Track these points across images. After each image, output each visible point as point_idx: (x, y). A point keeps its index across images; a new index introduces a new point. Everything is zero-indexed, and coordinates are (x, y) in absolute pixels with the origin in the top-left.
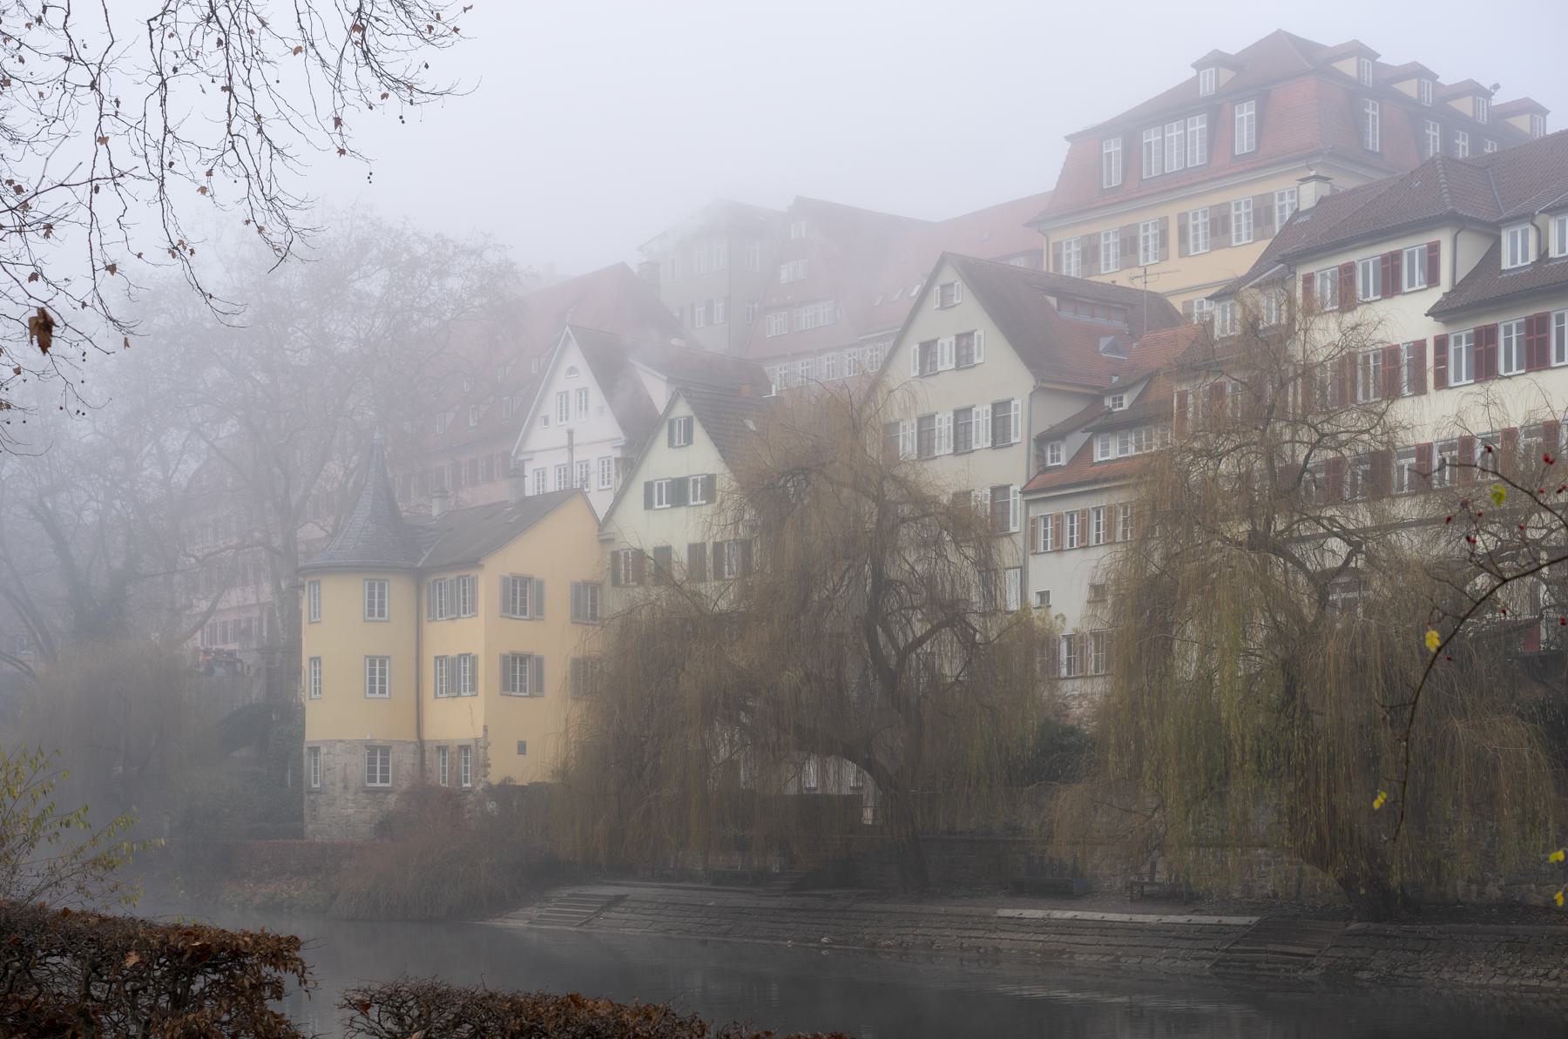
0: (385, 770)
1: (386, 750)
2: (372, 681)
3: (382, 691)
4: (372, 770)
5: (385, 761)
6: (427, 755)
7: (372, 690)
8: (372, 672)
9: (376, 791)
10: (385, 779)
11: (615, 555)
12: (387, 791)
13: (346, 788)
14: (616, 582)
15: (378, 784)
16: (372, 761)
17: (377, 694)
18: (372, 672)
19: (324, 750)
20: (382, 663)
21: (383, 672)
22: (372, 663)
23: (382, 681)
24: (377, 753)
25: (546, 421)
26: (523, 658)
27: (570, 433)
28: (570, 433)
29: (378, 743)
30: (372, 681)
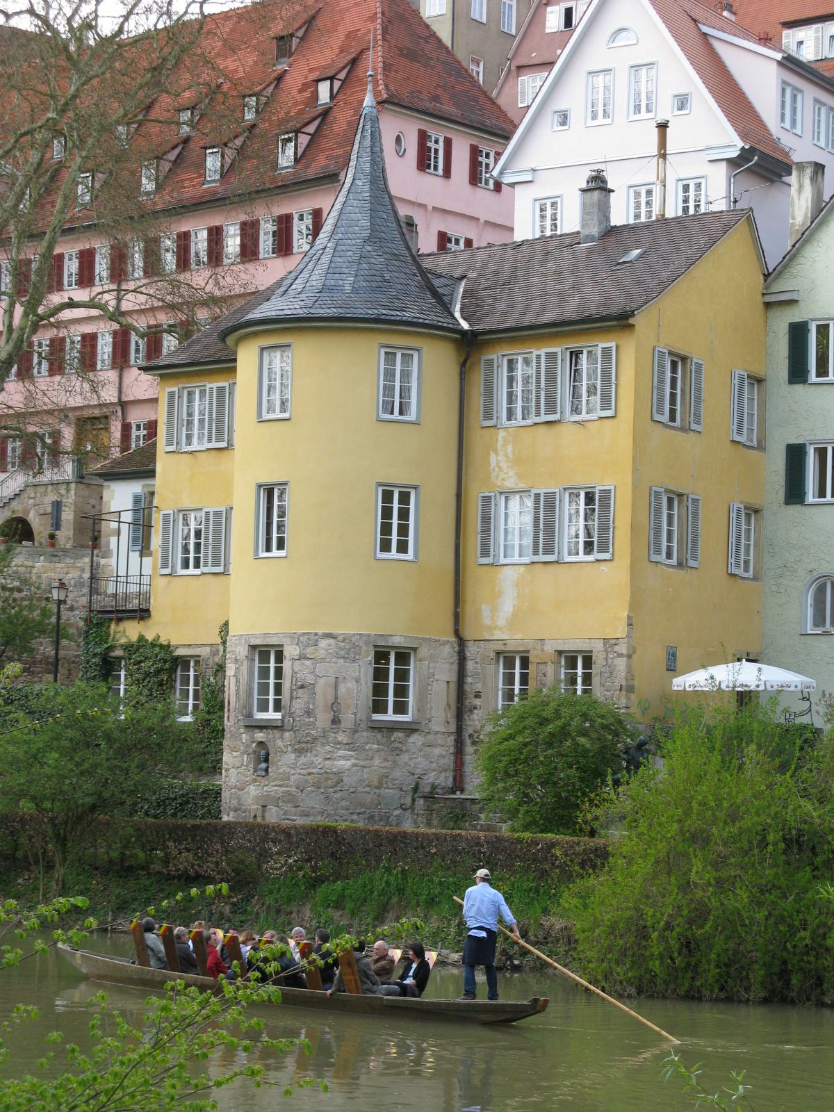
0: (401, 691)
1: (403, 657)
2: (386, 529)
3: (403, 547)
4: (379, 690)
5: (402, 676)
6: (470, 665)
7: (386, 546)
8: (387, 513)
9: (392, 728)
10: (400, 708)
11: (798, 332)
12: (410, 729)
13: (336, 721)
14: (797, 373)
15: (390, 716)
16: (380, 674)
17: (394, 554)
18: (387, 513)
19: (290, 651)
20: (404, 498)
21: (404, 514)
22: (387, 496)
23: (403, 530)
24: (389, 663)
25: (564, 119)
26: (675, 497)
27: (663, 127)
28: (663, 127)
29: (397, 641)
30: (386, 529)
